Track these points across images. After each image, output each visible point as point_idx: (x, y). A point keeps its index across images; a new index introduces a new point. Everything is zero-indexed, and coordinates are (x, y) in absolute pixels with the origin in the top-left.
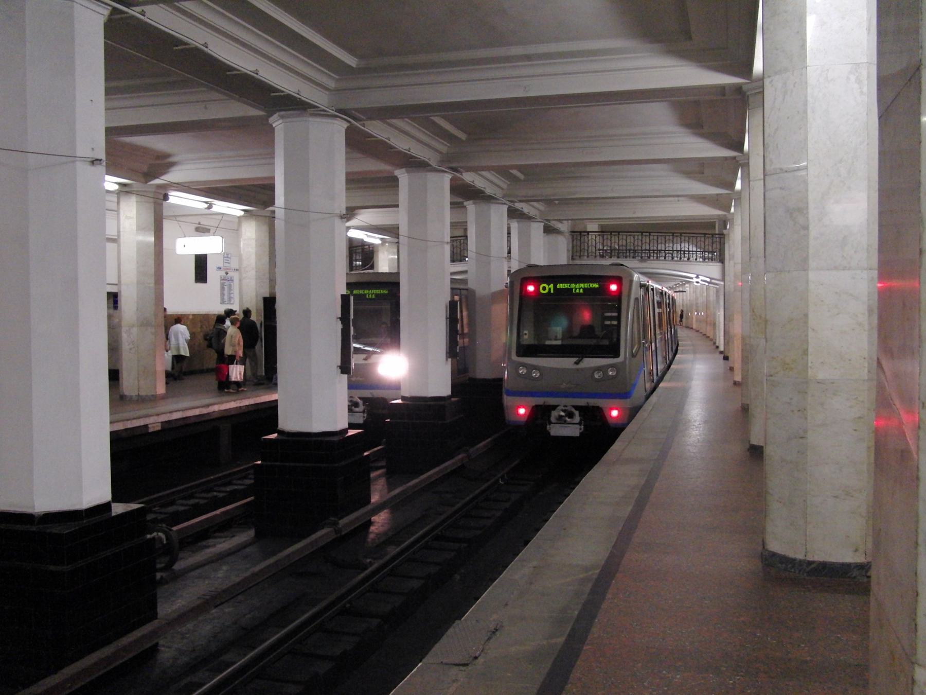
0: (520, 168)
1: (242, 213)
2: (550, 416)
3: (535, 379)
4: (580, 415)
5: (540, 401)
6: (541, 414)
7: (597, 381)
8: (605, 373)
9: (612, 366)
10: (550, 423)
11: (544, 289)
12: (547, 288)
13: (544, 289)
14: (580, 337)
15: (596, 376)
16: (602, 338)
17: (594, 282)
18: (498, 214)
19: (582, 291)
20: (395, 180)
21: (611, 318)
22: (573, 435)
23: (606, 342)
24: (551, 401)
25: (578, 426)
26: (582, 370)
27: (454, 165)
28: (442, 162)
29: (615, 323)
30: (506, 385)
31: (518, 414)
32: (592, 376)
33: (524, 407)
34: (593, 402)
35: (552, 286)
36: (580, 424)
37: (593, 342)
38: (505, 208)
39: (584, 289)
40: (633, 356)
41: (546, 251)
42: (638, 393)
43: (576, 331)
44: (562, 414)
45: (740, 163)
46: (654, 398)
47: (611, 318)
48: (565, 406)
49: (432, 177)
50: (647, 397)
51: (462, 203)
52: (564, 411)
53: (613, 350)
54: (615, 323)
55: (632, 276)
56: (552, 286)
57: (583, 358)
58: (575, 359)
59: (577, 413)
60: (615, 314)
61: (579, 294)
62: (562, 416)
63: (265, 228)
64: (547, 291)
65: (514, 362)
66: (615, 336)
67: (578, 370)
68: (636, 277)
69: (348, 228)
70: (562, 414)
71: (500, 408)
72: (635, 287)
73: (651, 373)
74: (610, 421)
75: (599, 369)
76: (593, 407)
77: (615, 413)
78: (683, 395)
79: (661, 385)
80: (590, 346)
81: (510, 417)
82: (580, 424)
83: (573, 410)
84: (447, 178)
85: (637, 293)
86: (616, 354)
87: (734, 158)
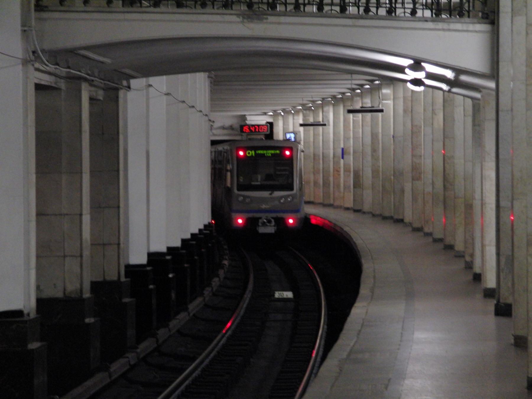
5: (251, 215)
9: (288, 196)
11: (249, 153)
13: (249, 153)
15: (282, 201)
17: (276, 150)
19: (270, 155)
24: (257, 215)
25: (274, 227)
34: (280, 215)
35: (253, 152)
36: (274, 226)
39: (272, 154)
44: (265, 221)
52: (266, 219)
58: (269, 192)
59: (273, 220)
61: (269, 157)
62: (264, 222)
67: (271, 198)
70: (265, 221)
74: (289, 225)
75: (282, 197)
76: (279, 218)
82: (274, 226)
86: (292, 189)
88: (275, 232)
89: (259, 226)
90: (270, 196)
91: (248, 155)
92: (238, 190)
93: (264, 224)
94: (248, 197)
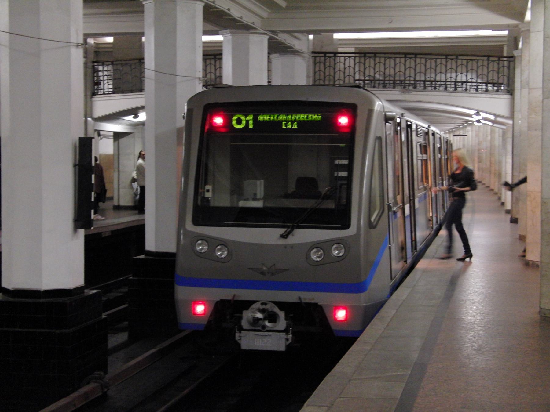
2: (241, 318)
3: (220, 260)
4: (286, 319)
5: (227, 294)
6: (227, 313)
7: (317, 264)
8: (327, 252)
9: (338, 241)
10: (241, 329)
11: (239, 121)
12: (243, 121)
13: (239, 121)
14: (293, 196)
15: (314, 257)
16: (327, 197)
17: (314, 112)
19: (295, 125)
21: (342, 168)
22: (275, 349)
23: (330, 205)
24: (244, 294)
25: (283, 335)
26: (292, 246)
29: (344, 174)
30: (179, 271)
32: (308, 256)
33: (203, 303)
34: (309, 297)
35: (250, 117)
36: (286, 331)
37: (309, 204)
39: (300, 123)
40: (371, 226)
41: (251, 67)
42: (379, 282)
43: (292, 188)
44: (259, 315)
46: (402, 292)
47: (342, 168)
48: (265, 304)
50: (395, 287)
52: (262, 311)
53: (340, 218)
54: (344, 174)
56: (250, 117)
57: (293, 228)
58: (282, 231)
59: (282, 315)
60: (346, 162)
61: (292, 130)
62: (258, 319)
64: (242, 125)
65: (187, 233)
66: (344, 195)
67: (285, 246)
68: (378, 105)
70: (259, 315)
71: (169, 305)
72: (376, 120)
73: (403, 248)
74: (334, 327)
75: (317, 245)
76: (309, 305)
77: (341, 314)
80: (305, 210)
81: (184, 318)
82: (286, 331)
83: (276, 310)
85: (377, 127)
86: (347, 226)
88: (288, 347)
89: (241, 329)
90: (282, 242)
94: (224, 243)
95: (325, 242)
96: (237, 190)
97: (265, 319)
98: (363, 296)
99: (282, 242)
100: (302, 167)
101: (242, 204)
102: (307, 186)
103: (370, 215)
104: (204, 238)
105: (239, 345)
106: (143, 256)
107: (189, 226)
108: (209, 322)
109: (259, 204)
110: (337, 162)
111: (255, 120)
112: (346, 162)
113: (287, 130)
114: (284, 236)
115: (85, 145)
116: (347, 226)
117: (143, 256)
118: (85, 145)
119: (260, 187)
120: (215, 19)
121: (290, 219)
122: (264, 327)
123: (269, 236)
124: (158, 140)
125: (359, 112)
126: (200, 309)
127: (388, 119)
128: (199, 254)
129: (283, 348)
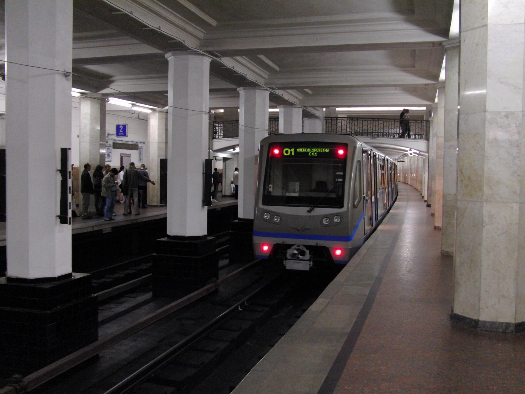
0: (266, 52)
1: (79, 95)
2: (286, 253)
3: (276, 223)
4: (310, 254)
5: (279, 240)
6: (279, 250)
7: (326, 226)
8: (332, 220)
9: (337, 214)
10: (286, 259)
11: (287, 152)
12: (289, 152)
13: (287, 152)
14: (314, 191)
15: (325, 222)
16: (332, 191)
18: (262, 97)
20: (166, 63)
21: (340, 176)
22: (303, 269)
23: (333, 196)
24: (288, 241)
25: (308, 262)
26: (313, 217)
27: (210, 49)
28: (201, 46)
29: (340, 180)
30: (255, 228)
31: (263, 250)
33: (267, 245)
35: (293, 150)
36: (309, 260)
37: (322, 195)
38: (267, 94)
39: (318, 153)
40: (355, 207)
41: (292, 124)
42: (358, 236)
43: (314, 186)
44: (296, 252)
45: (446, 47)
46: (370, 241)
47: (340, 176)
48: (299, 246)
49: (193, 60)
51: (235, 90)
52: (297, 250)
53: (339, 202)
54: (340, 180)
55: (355, 143)
57: (314, 207)
58: (308, 209)
59: (307, 252)
60: (341, 173)
61: (314, 157)
62: (295, 254)
63: (97, 107)
64: (289, 154)
66: (341, 190)
67: (310, 217)
68: (359, 144)
69: (108, 95)
70: (296, 252)
73: (371, 219)
74: (334, 258)
77: (338, 252)
78: (395, 237)
79: (380, 228)
81: (257, 253)
82: (309, 260)
83: (305, 249)
84: (206, 61)
85: (358, 156)
86: (342, 207)
87: (440, 44)
88: (310, 268)
89: (286, 259)
90: (308, 214)
91: (285, 154)
92: (264, 203)
93: (294, 257)
95: (330, 215)
96: (285, 188)
97: (299, 254)
98: (350, 242)
99: (308, 214)
100: (319, 176)
101: (288, 194)
102: (321, 186)
103: (354, 202)
104: (268, 212)
105: (285, 267)
106: (237, 221)
107: (261, 205)
108: (270, 255)
109: (297, 195)
110: (337, 173)
111: (295, 151)
112: (341, 173)
113: (312, 157)
114: (309, 211)
115: (208, 163)
116: (342, 207)
117: (237, 221)
118: (208, 163)
119: (297, 186)
120: (275, 100)
121: (313, 203)
122: (298, 258)
123: (302, 211)
124: (246, 162)
125: (349, 147)
126: (266, 248)
127: (364, 152)
128: (266, 220)
129: (307, 269)
